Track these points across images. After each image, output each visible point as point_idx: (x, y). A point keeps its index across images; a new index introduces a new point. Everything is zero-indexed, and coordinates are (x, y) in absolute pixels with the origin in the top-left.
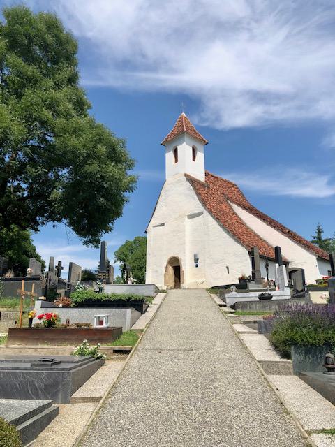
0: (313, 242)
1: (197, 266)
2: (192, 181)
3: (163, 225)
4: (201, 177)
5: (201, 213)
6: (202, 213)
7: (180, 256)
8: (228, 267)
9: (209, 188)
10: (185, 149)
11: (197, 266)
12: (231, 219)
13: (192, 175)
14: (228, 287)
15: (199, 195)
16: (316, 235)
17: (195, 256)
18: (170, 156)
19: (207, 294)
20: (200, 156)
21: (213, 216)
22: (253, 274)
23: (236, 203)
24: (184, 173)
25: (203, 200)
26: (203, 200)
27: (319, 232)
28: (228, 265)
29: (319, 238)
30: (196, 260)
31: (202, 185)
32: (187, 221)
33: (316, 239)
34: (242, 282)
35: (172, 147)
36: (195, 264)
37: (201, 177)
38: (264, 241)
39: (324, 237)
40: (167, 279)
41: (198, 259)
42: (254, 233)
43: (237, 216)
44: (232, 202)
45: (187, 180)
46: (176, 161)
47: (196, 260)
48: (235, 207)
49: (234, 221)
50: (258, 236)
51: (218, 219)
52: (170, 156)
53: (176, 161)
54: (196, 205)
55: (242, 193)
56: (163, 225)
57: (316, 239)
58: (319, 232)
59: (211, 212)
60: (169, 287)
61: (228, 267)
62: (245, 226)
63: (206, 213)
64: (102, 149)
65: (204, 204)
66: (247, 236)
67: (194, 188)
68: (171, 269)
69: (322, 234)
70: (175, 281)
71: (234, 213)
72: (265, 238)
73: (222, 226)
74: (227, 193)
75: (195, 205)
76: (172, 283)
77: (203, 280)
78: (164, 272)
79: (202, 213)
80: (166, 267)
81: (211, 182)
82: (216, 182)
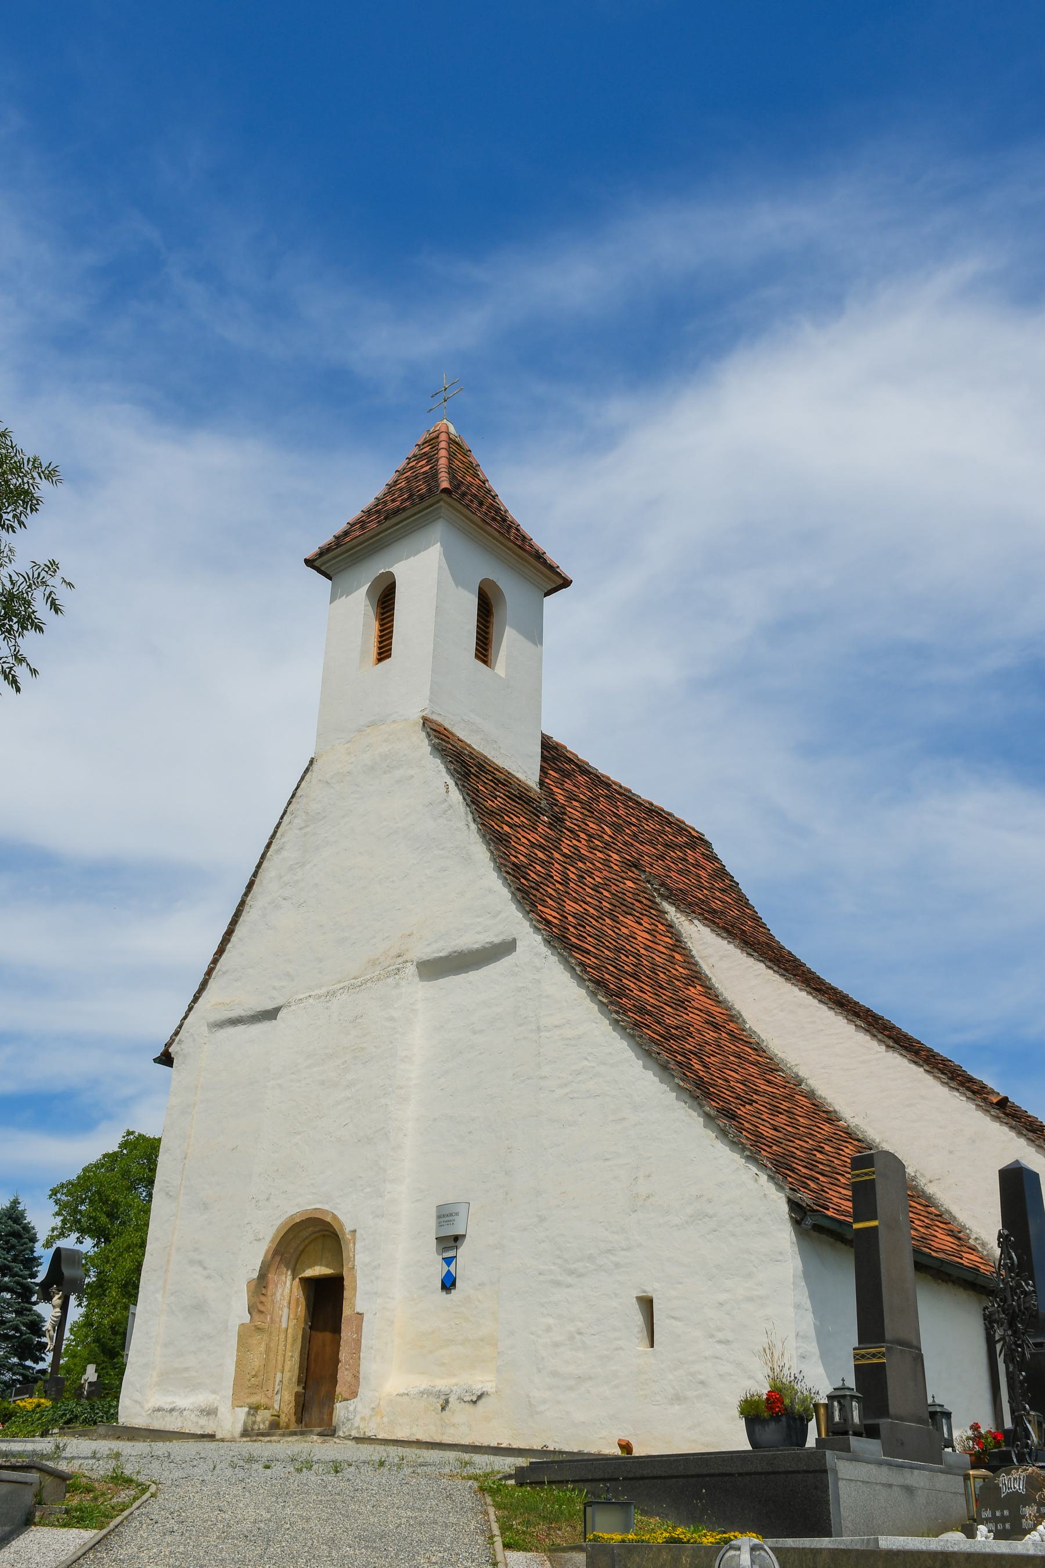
1: (449, 1284)
3: (270, 1015)
6: (506, 948)
8: (647, 1304)
9: (557, 820)
11: (449, 1284)
13: (461, 732)
17: (445, 1215)
28: (651, 1289)
31: (520, 796)
34: (771, 1433)
36: (437, 1270)
40: (256, 1361)
41: (457, 1239)
42: (811, 1095)
43: (710, 991)
46: (384, 652)
50: (831, 1117)
53: (384, 652)
56: (270, 1015)
60: (263, 1418)
61: (647, 1304)
66: (775, 1111)
67: (474, 801)
71: (696, 976)
74: (658, 869)
77: (482, 1380)
78: (239, 1311)
79: (506, 948)
80: (261, 1284)
81: (571, 797)
82: (603, 805)
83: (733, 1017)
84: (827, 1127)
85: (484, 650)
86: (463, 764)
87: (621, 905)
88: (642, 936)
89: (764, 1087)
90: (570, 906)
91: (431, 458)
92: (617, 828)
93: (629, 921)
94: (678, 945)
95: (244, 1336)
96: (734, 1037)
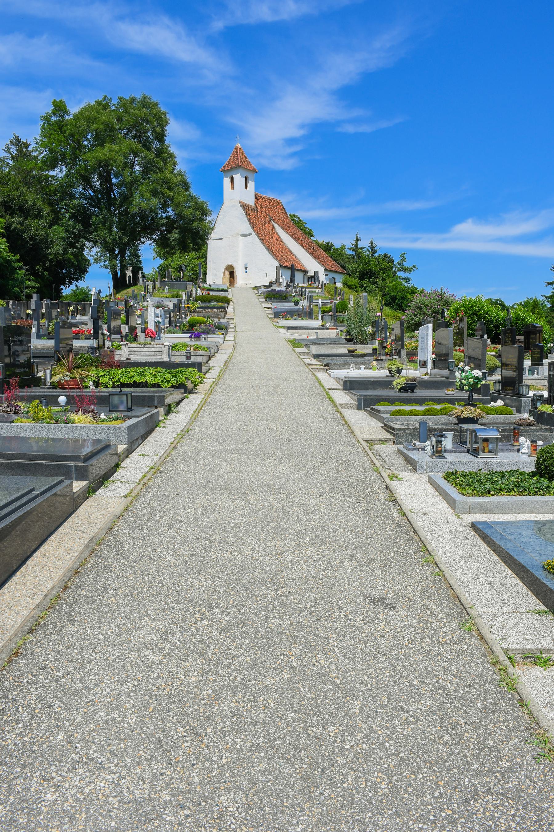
0: (350, 249)
1: (246, 272)
2: (245, 207)
3: (222, 239)
4: (251, 202)
5: (251, 234)
6: (251, 234)
7: (234, 264)
10: (239, 178)
11: (246, 272)
12: (272, 238)
14: (260, 286)
15: (249, 219)
16: (354, 242)
17: (245, 265)
18: (227, 181)
19: (252, 290)
20: (251, 184)
21: (259, 237)
22: (276, 280)
23: (278, 225)
24: (238, 199)
25: (252, 223)
26: (252, 223)
27: (357, 240)
29: (356, 246)
30: (246, 268)
31: (252, 210)
32: (241, 239)
33: (353, 246)
35: (230, 174)
37: (251, 202)
38: (294, 255)
39: (360, 245)
42: (288, 249)
44: (275, 222)
45: (241, 206)
46: (232, 188)
47: (246, 268)
48: (276, 226)
49: (274, 239)
51: (262, 240)
52: (227, 181)
53: (232, 188)
54: (247, 228)
55: (285, 211)
56: (222, 239)
57: (353, 246)
58: (357, 240)
59: (258, 234)
62: (283, 242)
63: (254, 234)
64: (198, 214)
65: (253, 228)
68: (227, 274)
69: (359, 242)
70: (230, 282)
71: (276, 232)
72: (295, 253)
73: (264, 246)
75: (247, 227)
76: (228, 283)
83: (280, 238)
84: (289, 253)
85: (246, 188)
86: (244, 207)
87: (266, 223)
88: (268, 227)
89: (281, 249)
90: (259, 226)
91: (236, 152)
92: (266, 208)
93: (266, 225)
94: (273, 227)
95: (223, 278)
96: (279, 241)
